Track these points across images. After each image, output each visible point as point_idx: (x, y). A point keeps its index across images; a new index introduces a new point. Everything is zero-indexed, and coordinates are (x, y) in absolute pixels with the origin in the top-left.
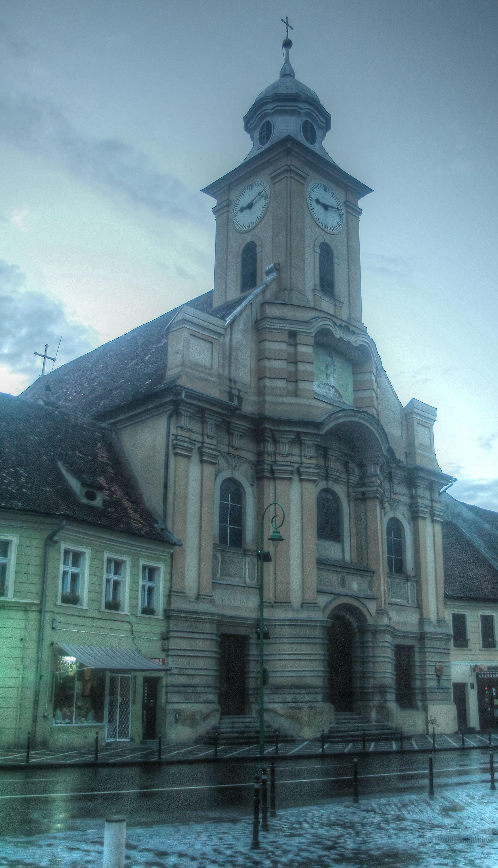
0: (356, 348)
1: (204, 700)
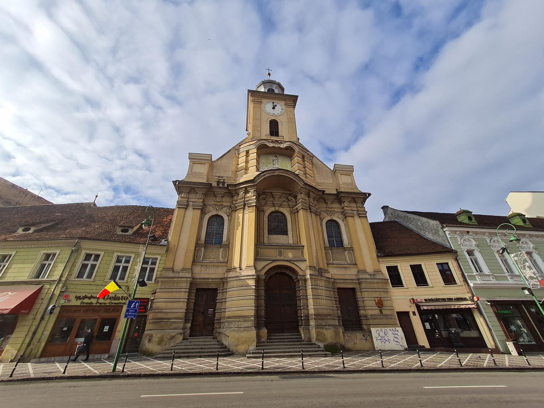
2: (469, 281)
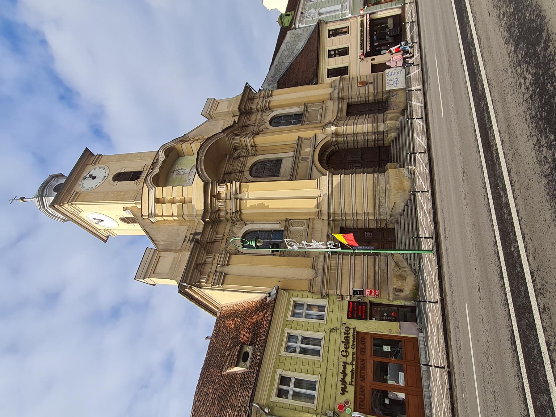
0: (167, 156)
2: (347, 17)
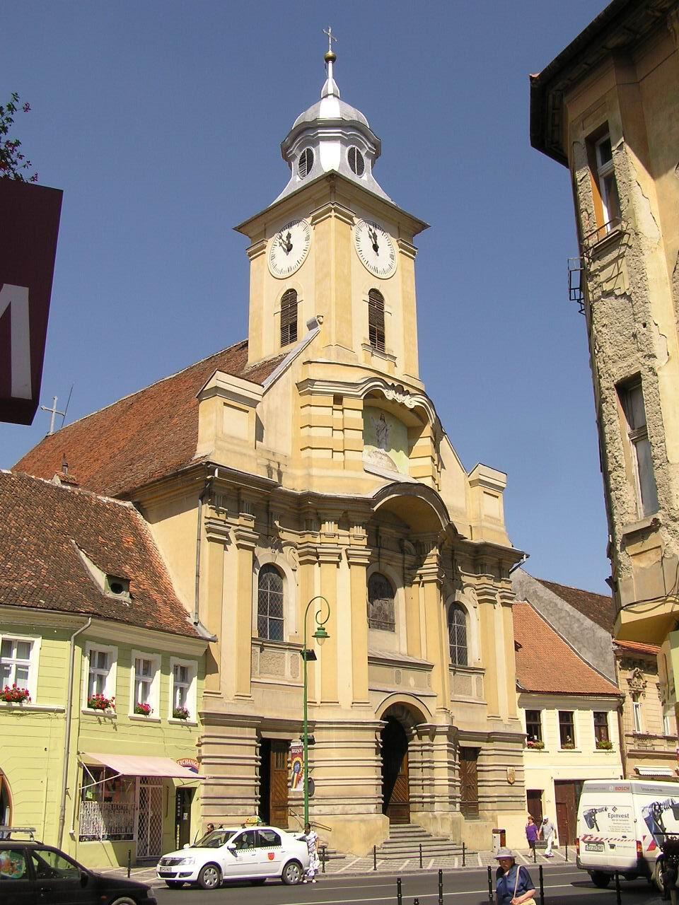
0: (412, 410)
1: (243, 813)
